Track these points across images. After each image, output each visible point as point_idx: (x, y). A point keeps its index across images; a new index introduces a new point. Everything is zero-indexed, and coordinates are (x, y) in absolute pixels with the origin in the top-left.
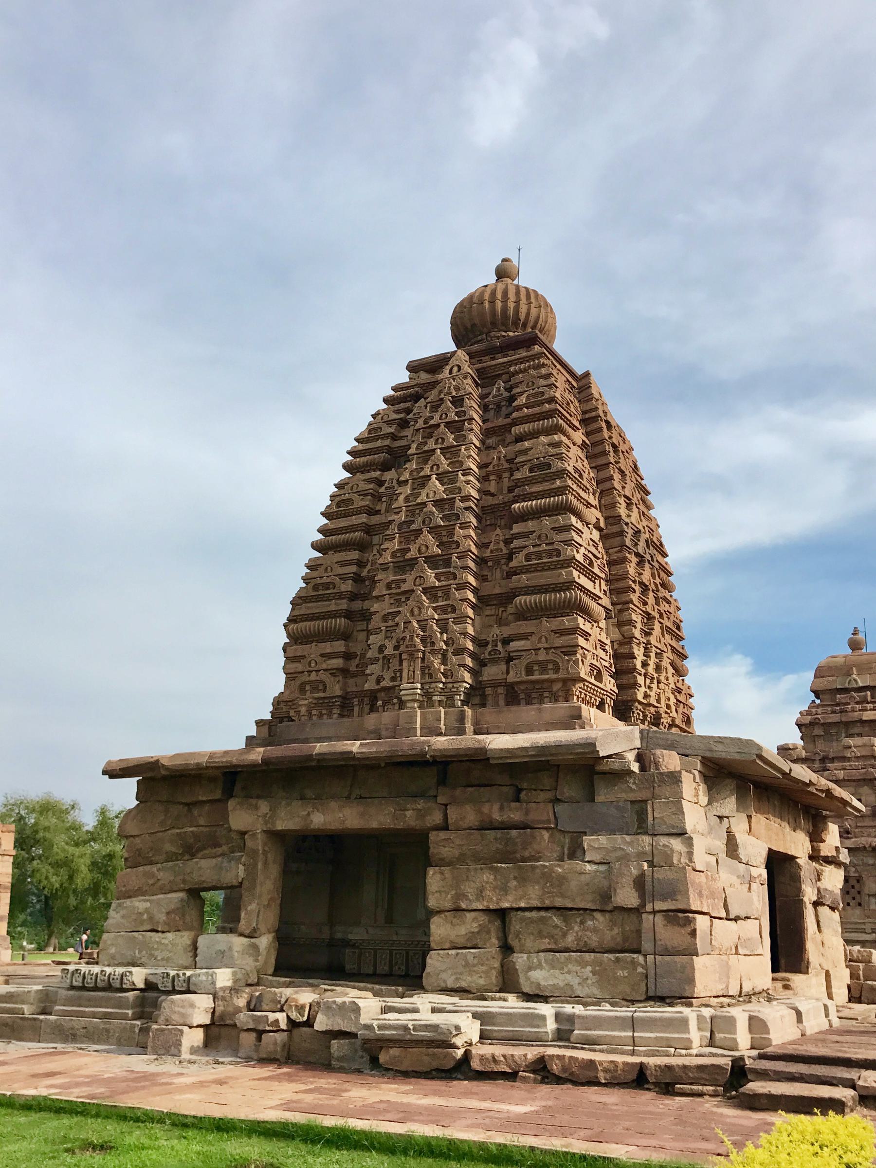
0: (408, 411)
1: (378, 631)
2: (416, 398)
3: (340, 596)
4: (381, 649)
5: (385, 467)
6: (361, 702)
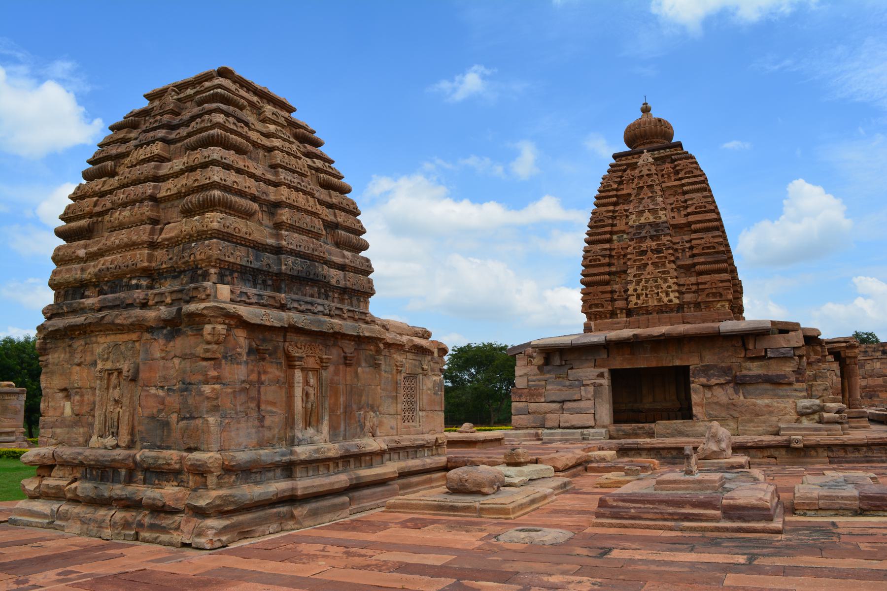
0: (621, 177)
1: (631, 282)
2: (625, 171)
3: (603, 265)
4: (635, 290)
5: (615, 204)
6: (621, 312)
